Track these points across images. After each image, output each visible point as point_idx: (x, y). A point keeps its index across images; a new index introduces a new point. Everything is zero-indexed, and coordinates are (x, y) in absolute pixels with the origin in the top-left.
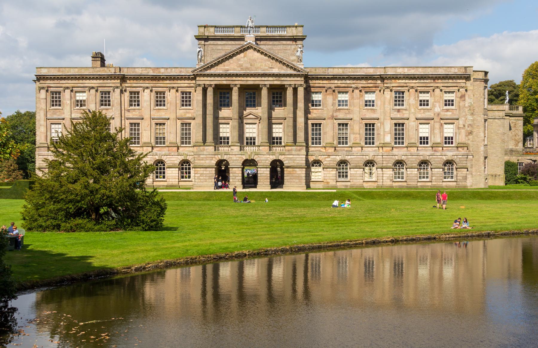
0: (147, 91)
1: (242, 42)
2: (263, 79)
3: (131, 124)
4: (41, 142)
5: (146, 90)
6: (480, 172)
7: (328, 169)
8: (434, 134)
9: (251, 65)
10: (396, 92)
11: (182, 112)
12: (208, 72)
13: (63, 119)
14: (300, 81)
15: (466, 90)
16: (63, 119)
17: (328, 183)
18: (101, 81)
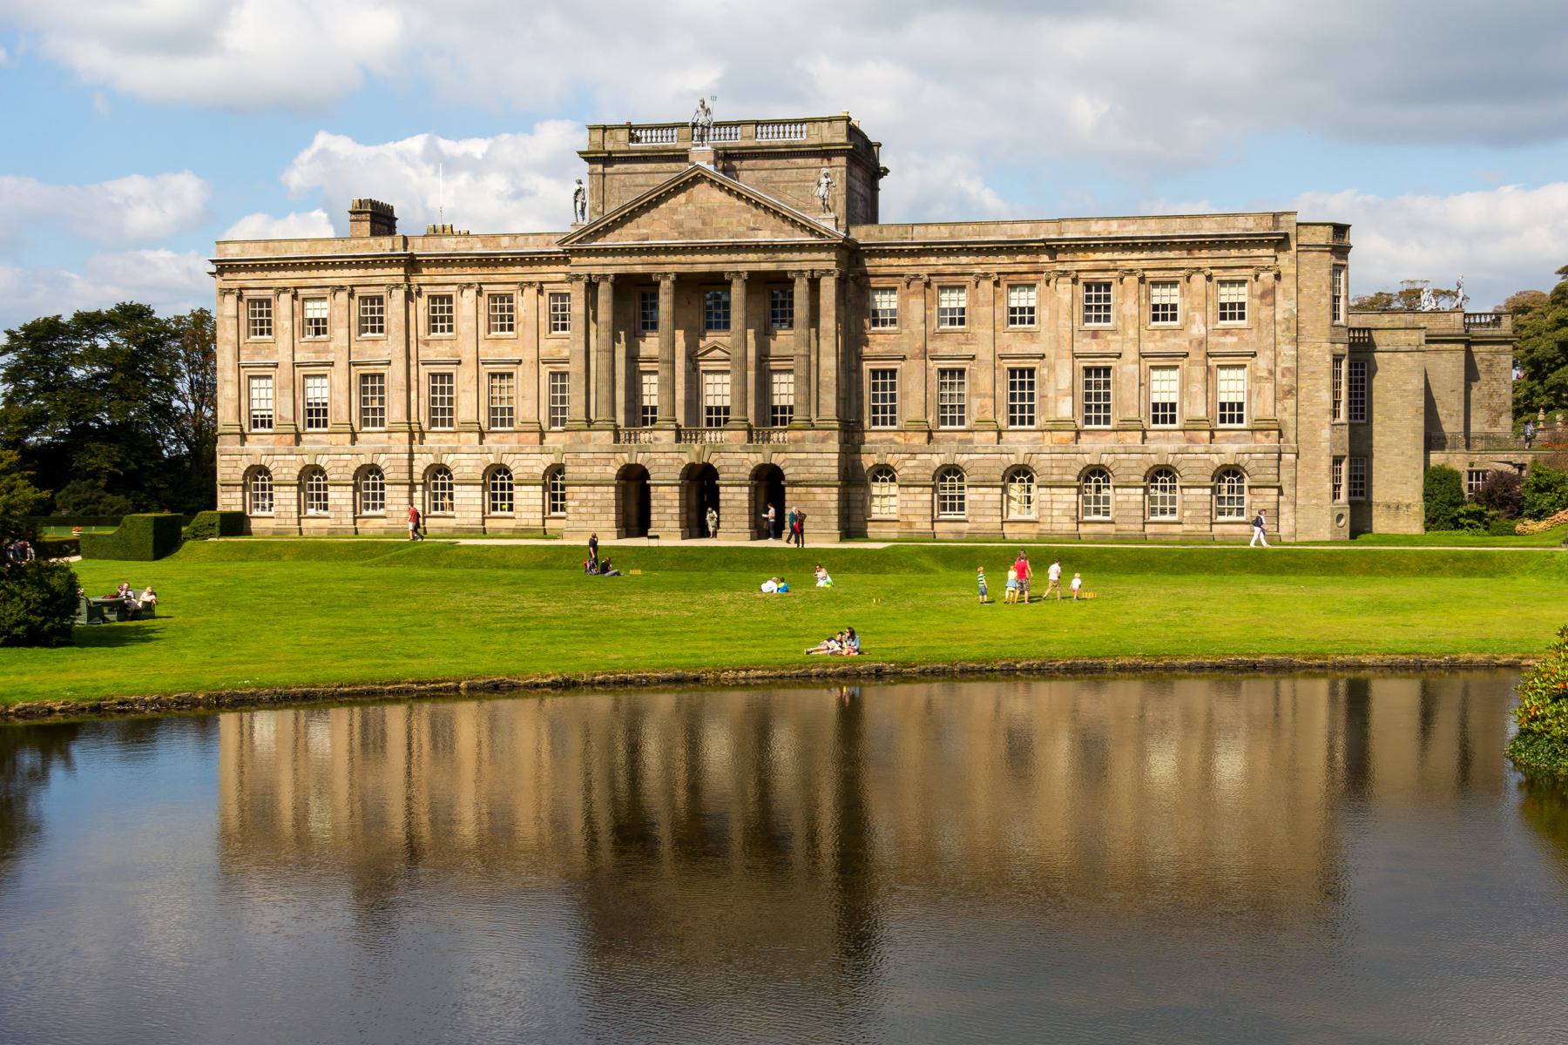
0: (470, 294)
1: (682, 165)
2: (734, 257)
3: (434, 376)
4: (226, 421)
5: (527, 290)
6: (1318, 497)
7: (911, 490)
8: (1190, 395)
9: (704, 223)
10: (1088, 286)
11: (552, 345)
12: (599, 243)
13: (276, 366)
14: (826, 262)
15: (1278, 277)
16: (276, 366)
17: (910, 524)
18: (361, 272)
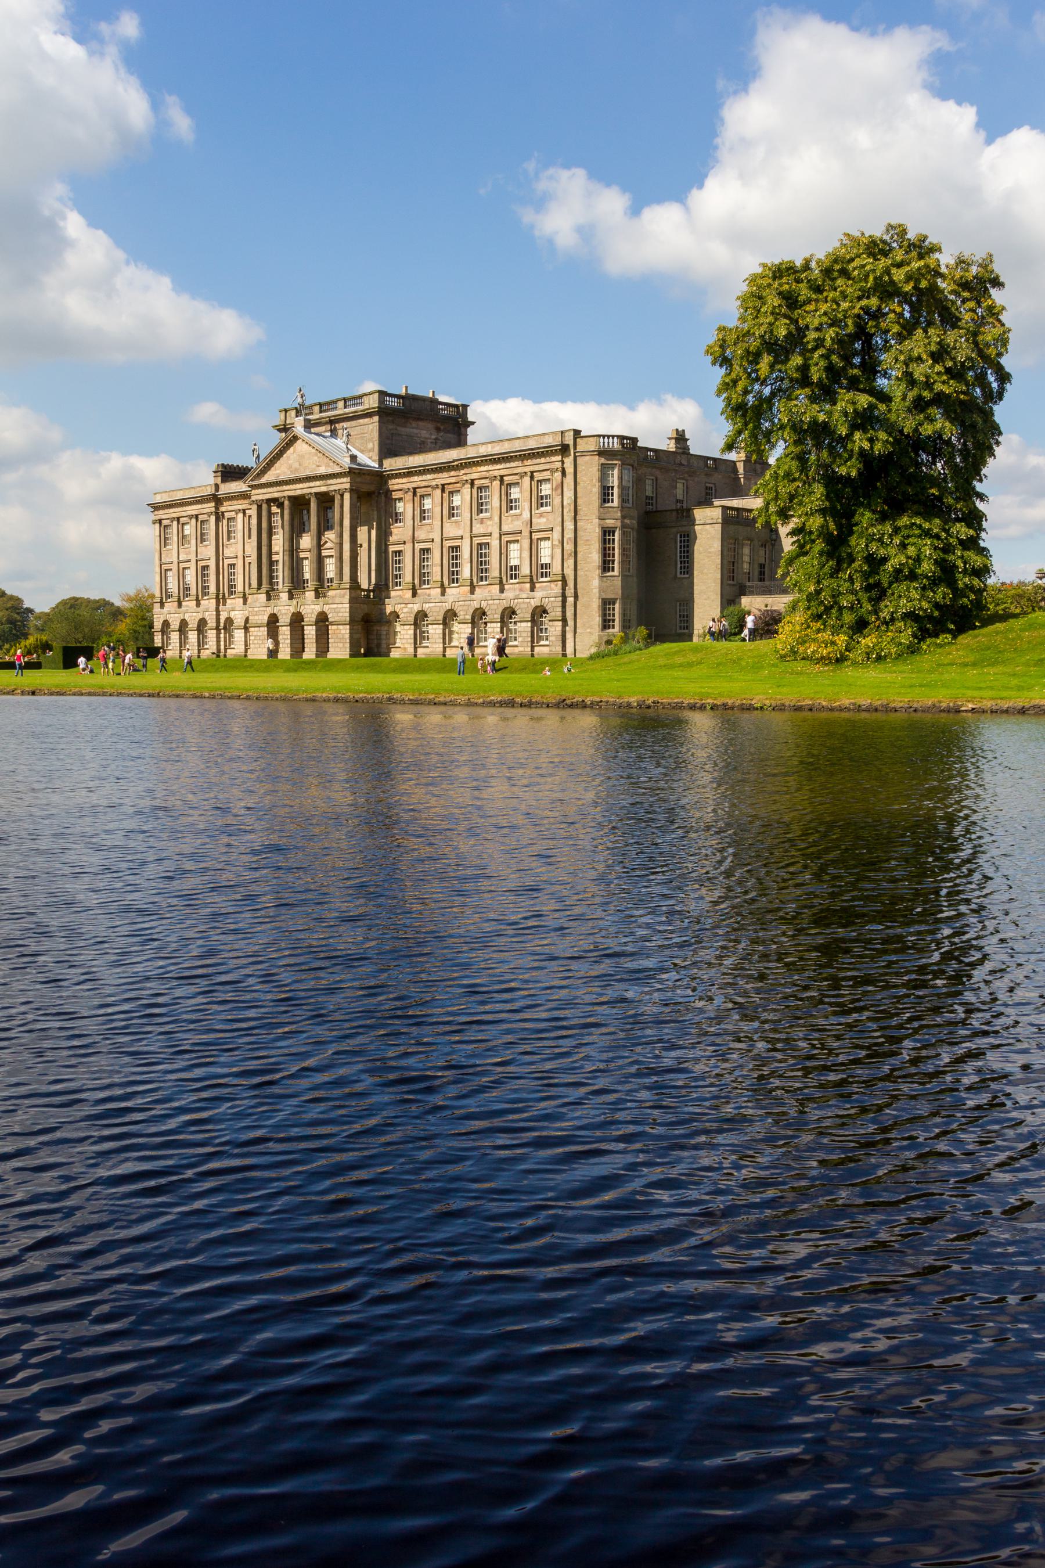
6: (591, 627)
18: (199, 506)
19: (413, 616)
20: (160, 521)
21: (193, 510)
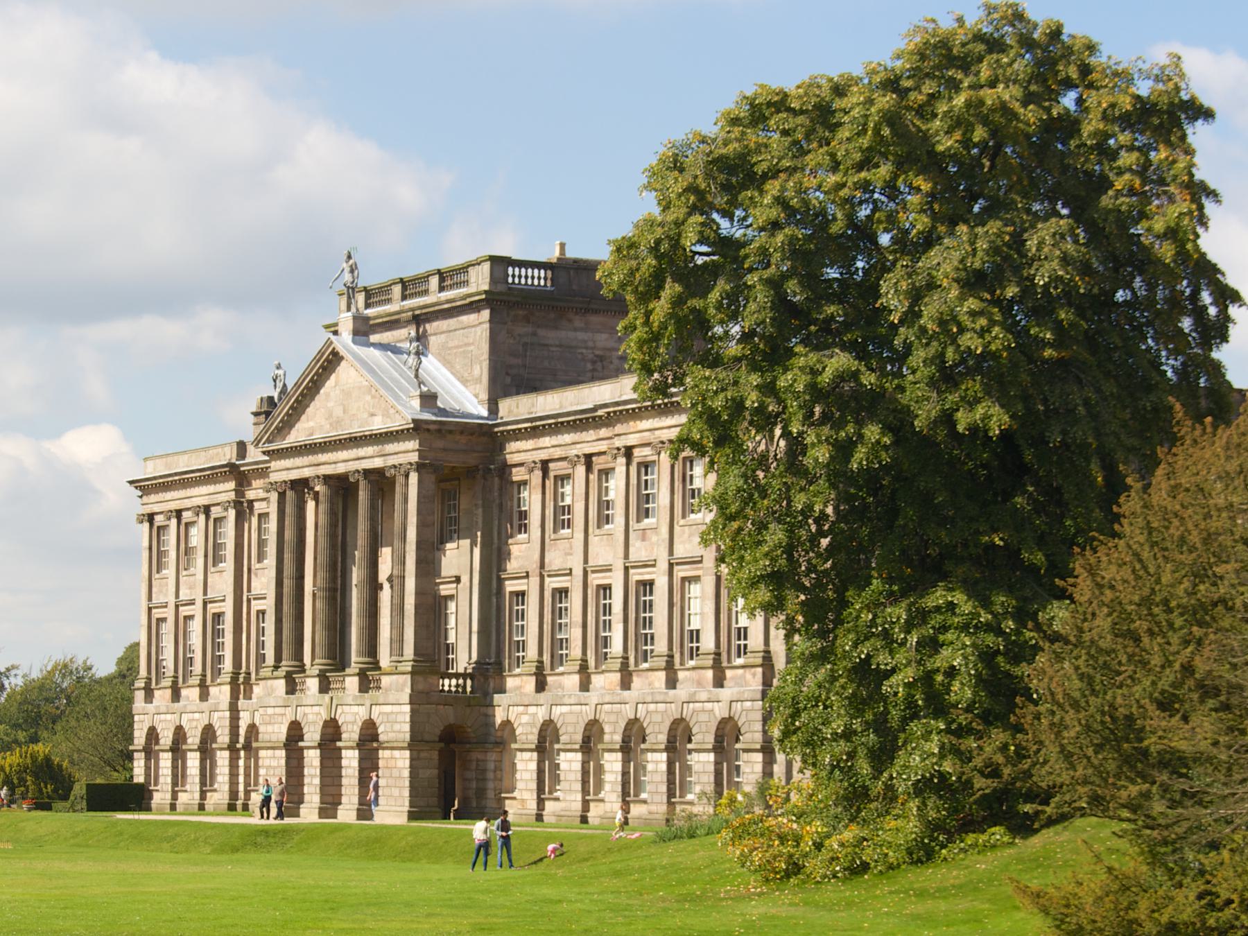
18: (211, 488)
19: (536, 731)
20: (151, 518)
21: (200, 495)
